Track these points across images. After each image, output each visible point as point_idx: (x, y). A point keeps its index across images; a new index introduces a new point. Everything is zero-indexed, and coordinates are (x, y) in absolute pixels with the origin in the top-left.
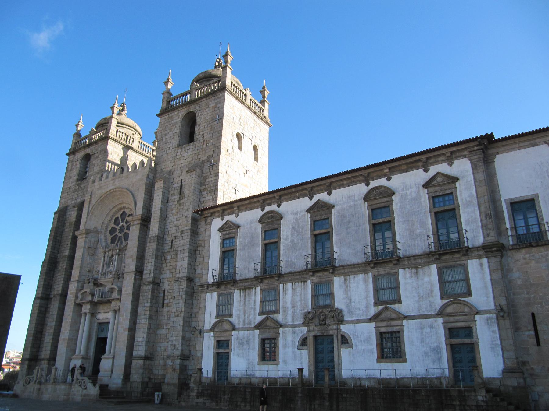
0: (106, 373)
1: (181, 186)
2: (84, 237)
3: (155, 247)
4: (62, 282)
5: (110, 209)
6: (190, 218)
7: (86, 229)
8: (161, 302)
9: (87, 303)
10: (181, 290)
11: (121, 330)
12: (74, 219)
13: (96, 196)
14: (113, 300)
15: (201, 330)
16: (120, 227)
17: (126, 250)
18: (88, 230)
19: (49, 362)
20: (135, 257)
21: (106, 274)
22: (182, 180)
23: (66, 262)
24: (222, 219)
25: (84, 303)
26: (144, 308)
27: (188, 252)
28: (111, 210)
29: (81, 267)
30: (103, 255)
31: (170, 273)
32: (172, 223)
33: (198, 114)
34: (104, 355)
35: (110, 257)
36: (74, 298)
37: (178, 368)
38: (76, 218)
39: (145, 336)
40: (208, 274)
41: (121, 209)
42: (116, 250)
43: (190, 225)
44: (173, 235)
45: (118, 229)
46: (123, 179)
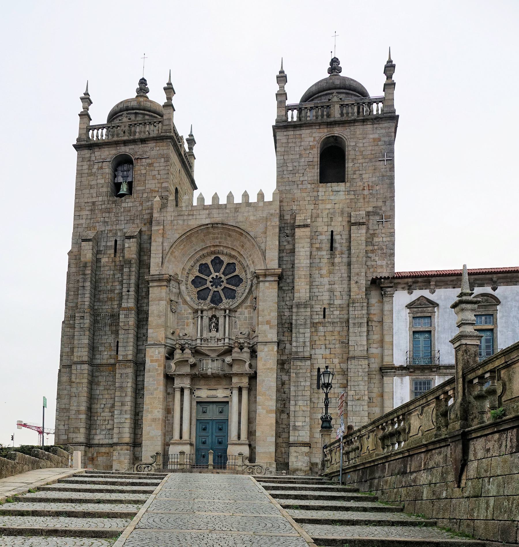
2: (164, 286)
3: (309, 314)
4: (132, 344)
5: (195, 250)
12: (134, 256)
13: (175, 227)
14: (237, 375)
16: (213, 278)
17: (237, 311)
18: (170, 276)
20: (275, 322)
21: (209, 340)
25: (179, 375)
29: (166, 327)
32: (322, 287)
44: (326, 302)
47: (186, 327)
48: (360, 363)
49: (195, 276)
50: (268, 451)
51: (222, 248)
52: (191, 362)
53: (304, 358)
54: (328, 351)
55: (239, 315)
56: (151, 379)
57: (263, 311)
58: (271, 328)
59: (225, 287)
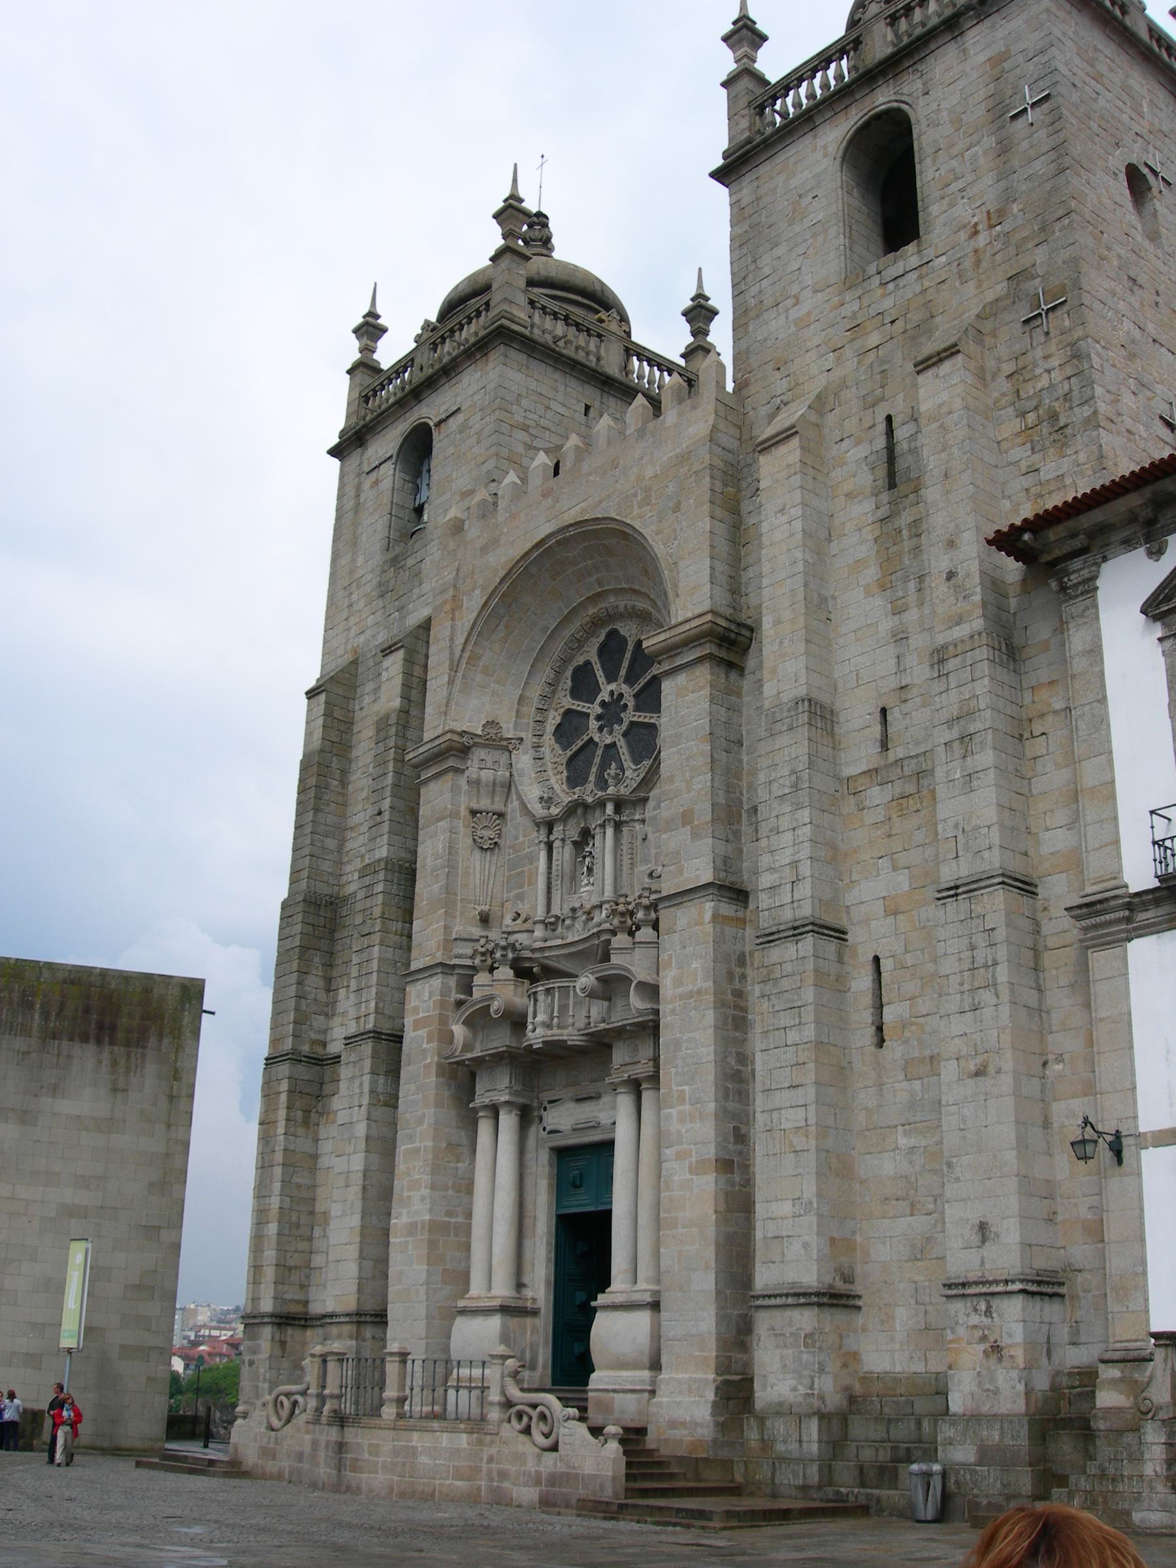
0: (625, 1373)
1: (890, 448)
5: (545, 629)
6: (977, 580)
7: (452, 731)
8: (866, 1016)
9: (497, 1059)
10: (980, 940)
11: (678, 1172)
14: (620, 1033)
15: (1118, 1135)
16: (603, 704)
17: (646, 800)
18: (462, 733)
19: (358, 1332)
20: (704, 813)
21: (568, 922)
22: (889, 419)
23: (380, 888)
24: (1157, 552)
26: (789, 1055)
27: (990, 744)
28: (550, 637)
29: (448, 900)
30: (543, 838)
31: (895, 869)
33: (920, 115)
34: (604, 1292)
35: (575, 843)
36: (435, 1044)
37: (1019, 1338)
38: (405, 697)
39: (809, 1188)
40: (1117, 842)
41: (596, 623)
42: (602, 804)
43: (979, 612)
45: (592, 717)
46: (592, 478)
47: (526, 888)
48: (978, 909)
49: (562, 710)
50: (694, 1331)
51: (612, 599)
52: (497, 1012)
53: (795, 928)
54: (903, 881)
55: (654, 809)
56: (412, 1087)
57: (671, 779)
58: (695, 836)
59: (632, 724)
